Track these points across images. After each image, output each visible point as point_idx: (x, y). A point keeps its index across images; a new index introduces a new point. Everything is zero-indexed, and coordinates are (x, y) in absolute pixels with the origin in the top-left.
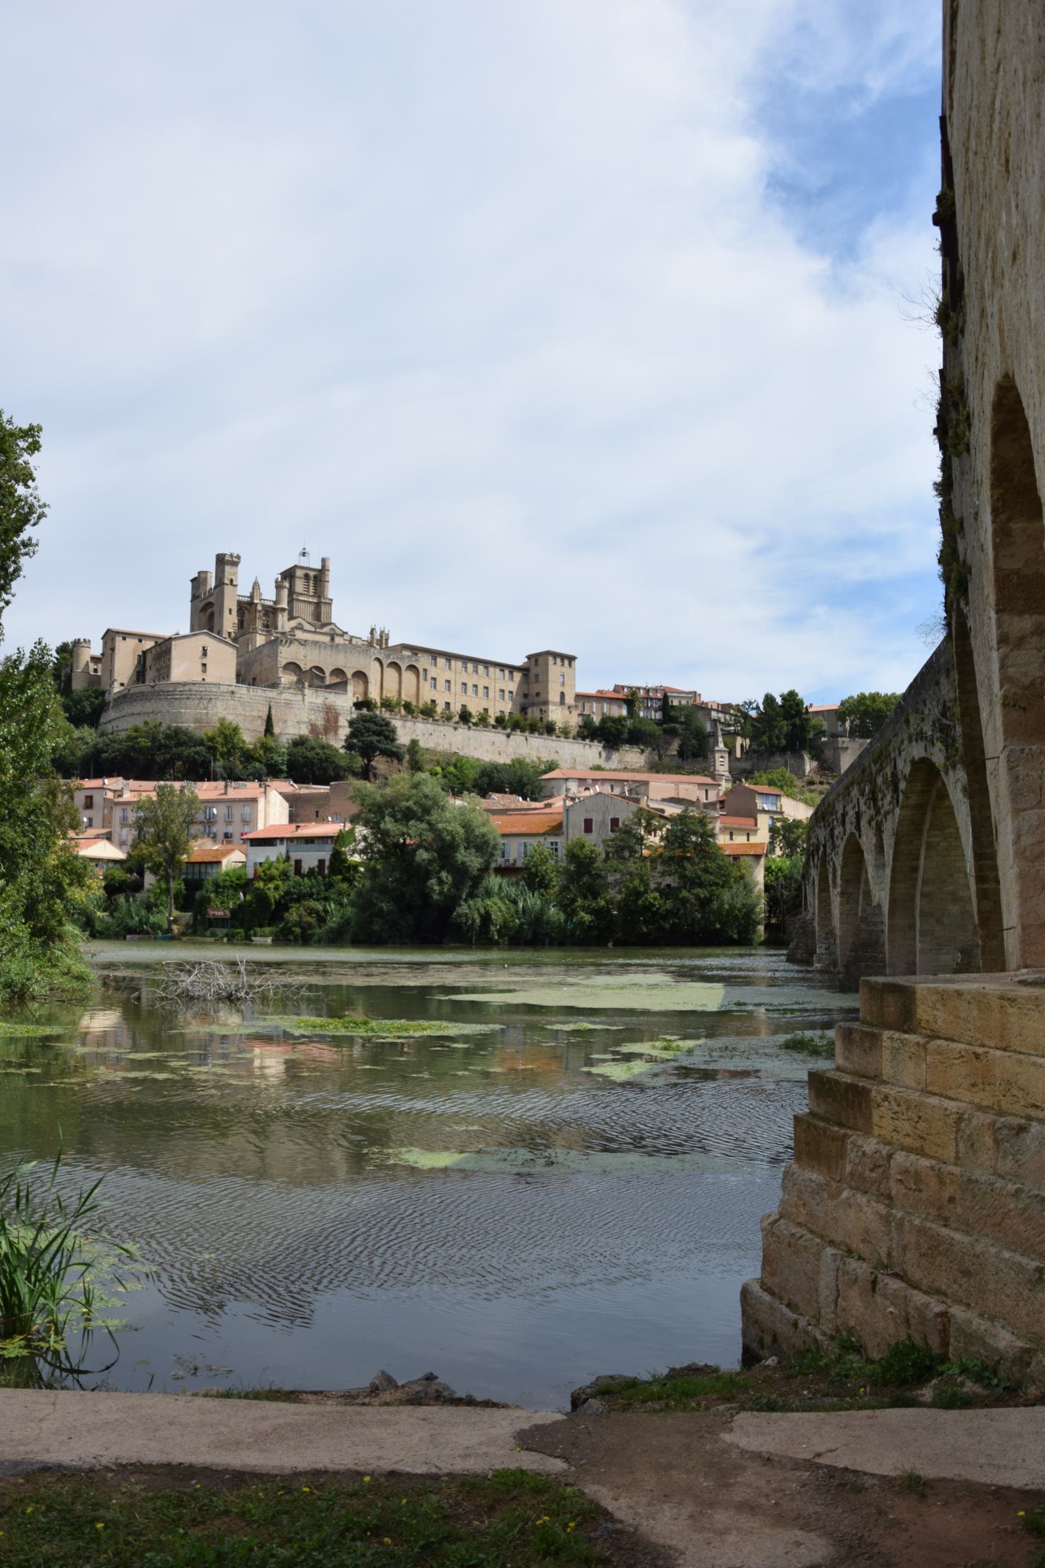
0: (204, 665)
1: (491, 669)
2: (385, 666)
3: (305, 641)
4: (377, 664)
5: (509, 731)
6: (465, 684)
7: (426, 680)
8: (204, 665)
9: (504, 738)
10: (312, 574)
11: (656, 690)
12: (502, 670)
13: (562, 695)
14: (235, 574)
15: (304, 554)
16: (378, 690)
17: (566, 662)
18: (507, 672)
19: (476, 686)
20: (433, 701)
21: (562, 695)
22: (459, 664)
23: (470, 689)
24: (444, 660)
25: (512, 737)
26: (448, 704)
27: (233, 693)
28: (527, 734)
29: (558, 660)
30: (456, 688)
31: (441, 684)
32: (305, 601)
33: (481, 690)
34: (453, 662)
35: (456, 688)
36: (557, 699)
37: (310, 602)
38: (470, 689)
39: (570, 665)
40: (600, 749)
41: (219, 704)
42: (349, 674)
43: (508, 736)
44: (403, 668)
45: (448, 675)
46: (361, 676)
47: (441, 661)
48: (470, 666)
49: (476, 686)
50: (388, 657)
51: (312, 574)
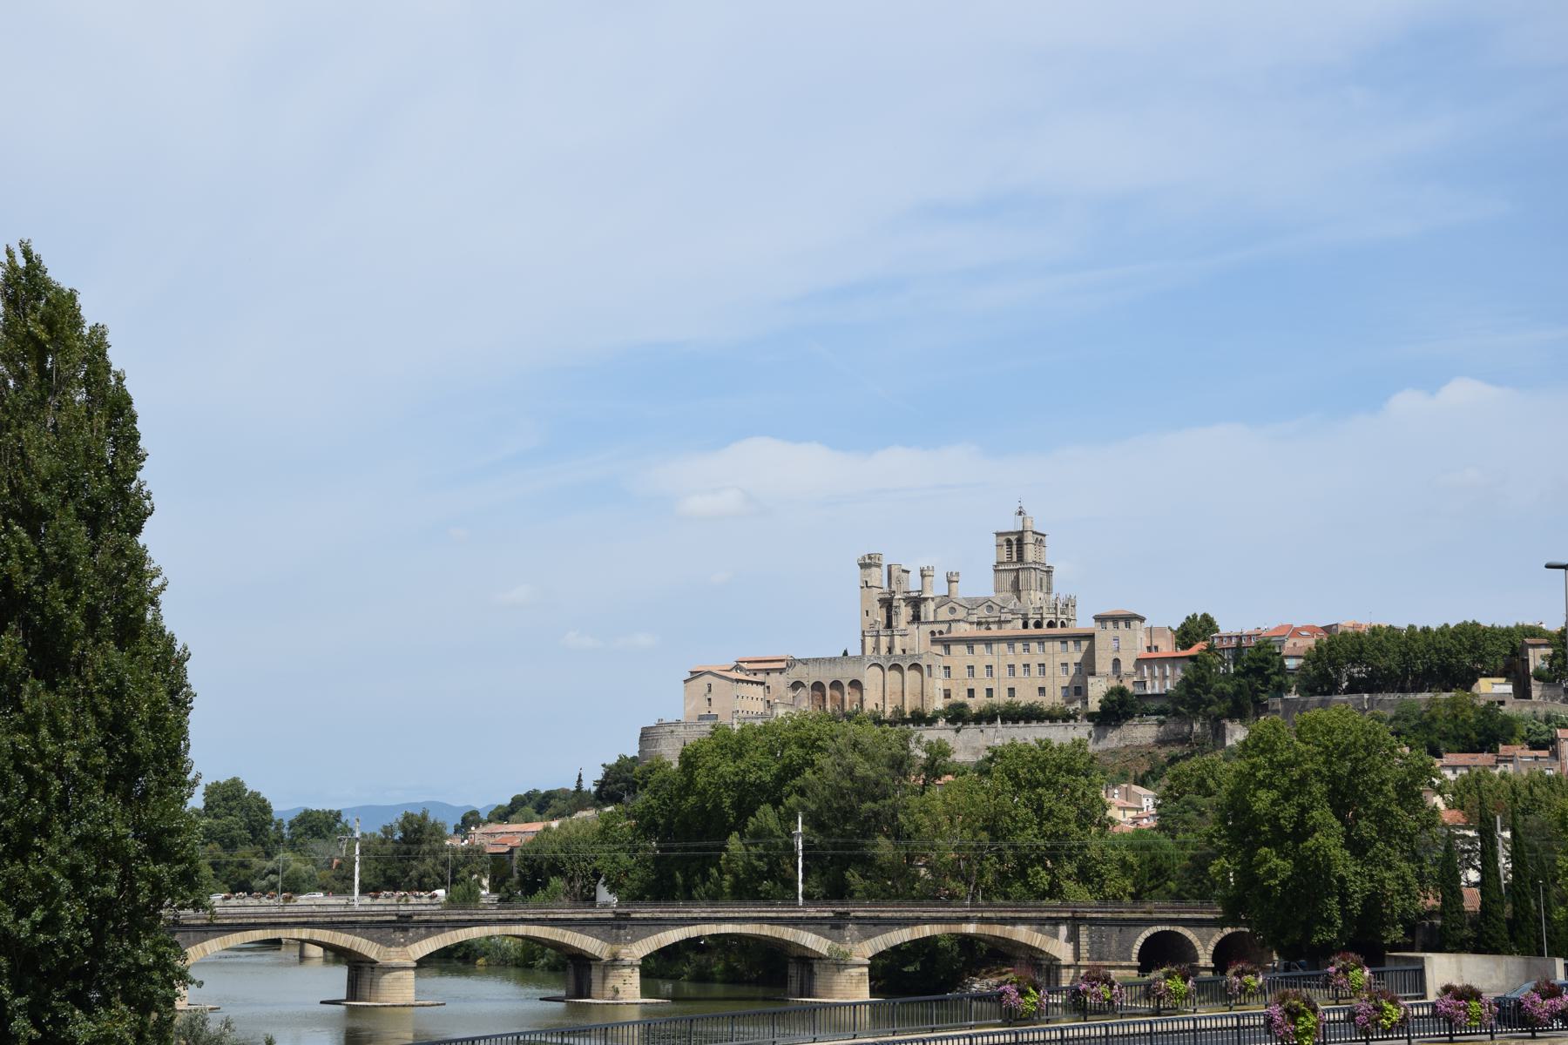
0: (709, 699)
1: (1048, 644)
2: (886, 670)
3: (807, 660)
4: (878, 669)
5: (960, 724)
6: (1011, 666)
7: (930, 675)
8: (709, 699)
9: (952, 734)
10: (1013, 538)
11: (1250, 636)
12: (1066, 642)
13: (1117, 662)
14: (869, 575)
15: (1020, 513)
16: (881, 695)
17: (1122, 624)
18: (1071, 643)
19: (1027, 666)
20: (971, 693)
21: (1117, 662)
22: (1004, 646)
23: (1020, 671)
24: (984, 646)
25: (962, 731)
26: (990, 692)
27: (672, 732)
28: (984, 725)
29: (1110, 625)
30: (1001, 671)
31: (980, 671)
32: (1005, 570)
33: (1035, 669)
34: (995, 647)
35: (1001, 671)
36: (1109, 668)
37: (1011, 570)
38: (1020, 671)
39: (1128, 625)
40: (1091, 728)
41: (663, 742)
42: (846, 683)
43: (958, 731)
44: (905, 668)
45: (989, 660)
46: (856, 684)
47: (980, 648)
48: (1019, 646)
49: (1027, 666)
50: (888, 661)
51: (1013, 538)
